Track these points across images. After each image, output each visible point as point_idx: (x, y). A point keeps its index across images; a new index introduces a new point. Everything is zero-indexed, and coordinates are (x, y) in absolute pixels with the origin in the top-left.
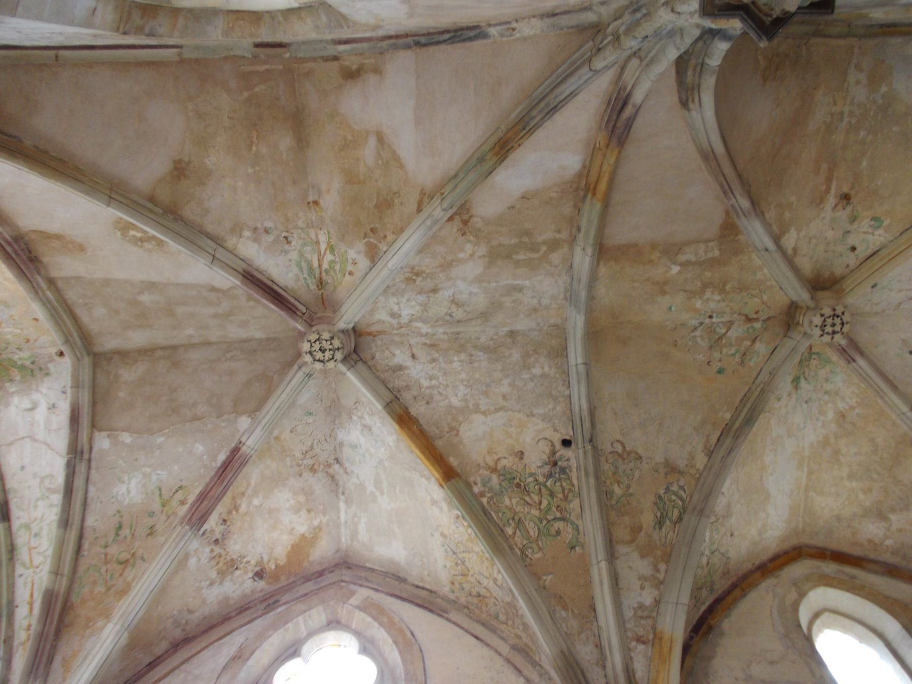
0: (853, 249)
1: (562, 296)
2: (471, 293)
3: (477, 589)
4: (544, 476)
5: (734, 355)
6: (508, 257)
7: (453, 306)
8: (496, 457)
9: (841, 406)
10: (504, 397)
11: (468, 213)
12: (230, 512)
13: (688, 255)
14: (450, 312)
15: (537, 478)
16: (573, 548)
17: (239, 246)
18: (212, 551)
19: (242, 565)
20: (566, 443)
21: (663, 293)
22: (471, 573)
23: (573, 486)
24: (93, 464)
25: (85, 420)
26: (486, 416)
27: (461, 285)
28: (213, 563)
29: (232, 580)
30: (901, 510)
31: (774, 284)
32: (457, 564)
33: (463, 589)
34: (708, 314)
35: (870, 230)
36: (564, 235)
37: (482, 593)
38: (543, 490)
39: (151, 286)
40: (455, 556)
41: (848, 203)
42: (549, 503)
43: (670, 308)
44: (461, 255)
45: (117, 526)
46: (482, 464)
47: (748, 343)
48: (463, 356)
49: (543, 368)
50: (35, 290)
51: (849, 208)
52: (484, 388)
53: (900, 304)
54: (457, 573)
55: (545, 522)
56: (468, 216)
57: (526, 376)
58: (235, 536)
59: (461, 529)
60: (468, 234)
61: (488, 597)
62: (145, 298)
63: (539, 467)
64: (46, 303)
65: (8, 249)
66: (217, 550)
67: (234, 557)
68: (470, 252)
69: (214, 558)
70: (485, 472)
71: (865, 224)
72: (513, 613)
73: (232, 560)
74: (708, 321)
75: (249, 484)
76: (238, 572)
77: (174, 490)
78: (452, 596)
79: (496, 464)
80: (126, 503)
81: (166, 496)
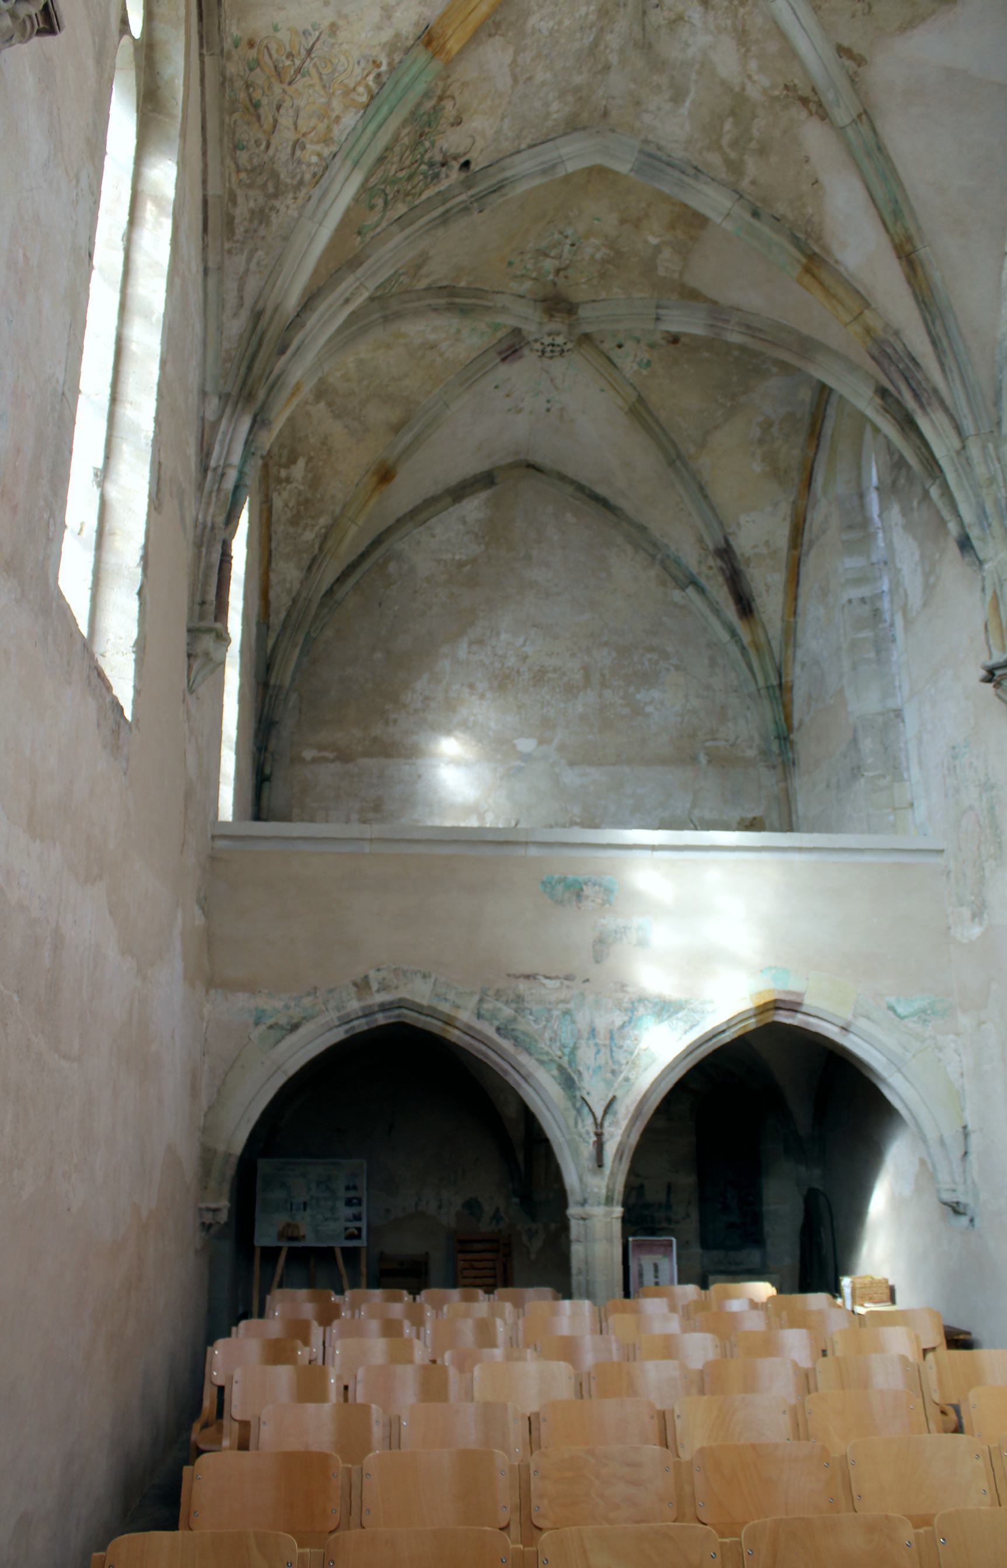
0: (620, 346)
1: (651, 137)
2: (687, 45)
3: (265, 101)
4: (431, 158)
5: (525, 268)
6: (733, 113)
7: (673, 16)
8: (456, 95)
9: (444, 346)
10: (530, 79)
11: (817, 113)
13: (666, 253)
14: (665, 8)
15: (429, 151)
16: (359, 233)
20: (466, 164)
21: (623, 221)
22: (290, 90)
23: (420, 194)
26: (510, 65)
27: (703, 39)
30: (332, 411)
31: (601, 297)
32: (290, 56)
33: (251, 70)
34: (577, 244)
35: (638, 359)
36: (745, 183)
37: (261, 111)
38: (416, 166)
40: (303, 53)
41: (668, 342)
42: (401, 179)
43: (598, 219)
44: (753, 65)
46: (449, 81)
47: (534, 275)
48: (592, 17)
49: (557, 112)
51: (663, 342)
52: (545, 52)
53: (547, 372)
54: (275, 56)
55: (382, 187)
56: (814, 110)
57: (551, 96)
59: (358, 71)
60: (785, 92)
61: (261, 126)
63: (441, 148)
68: (756, 77)
70: (440, 89)
71: (646, 356)
72: (265, 184)
74: (569, 242)
78: (228, 44)
79: (449, 97)
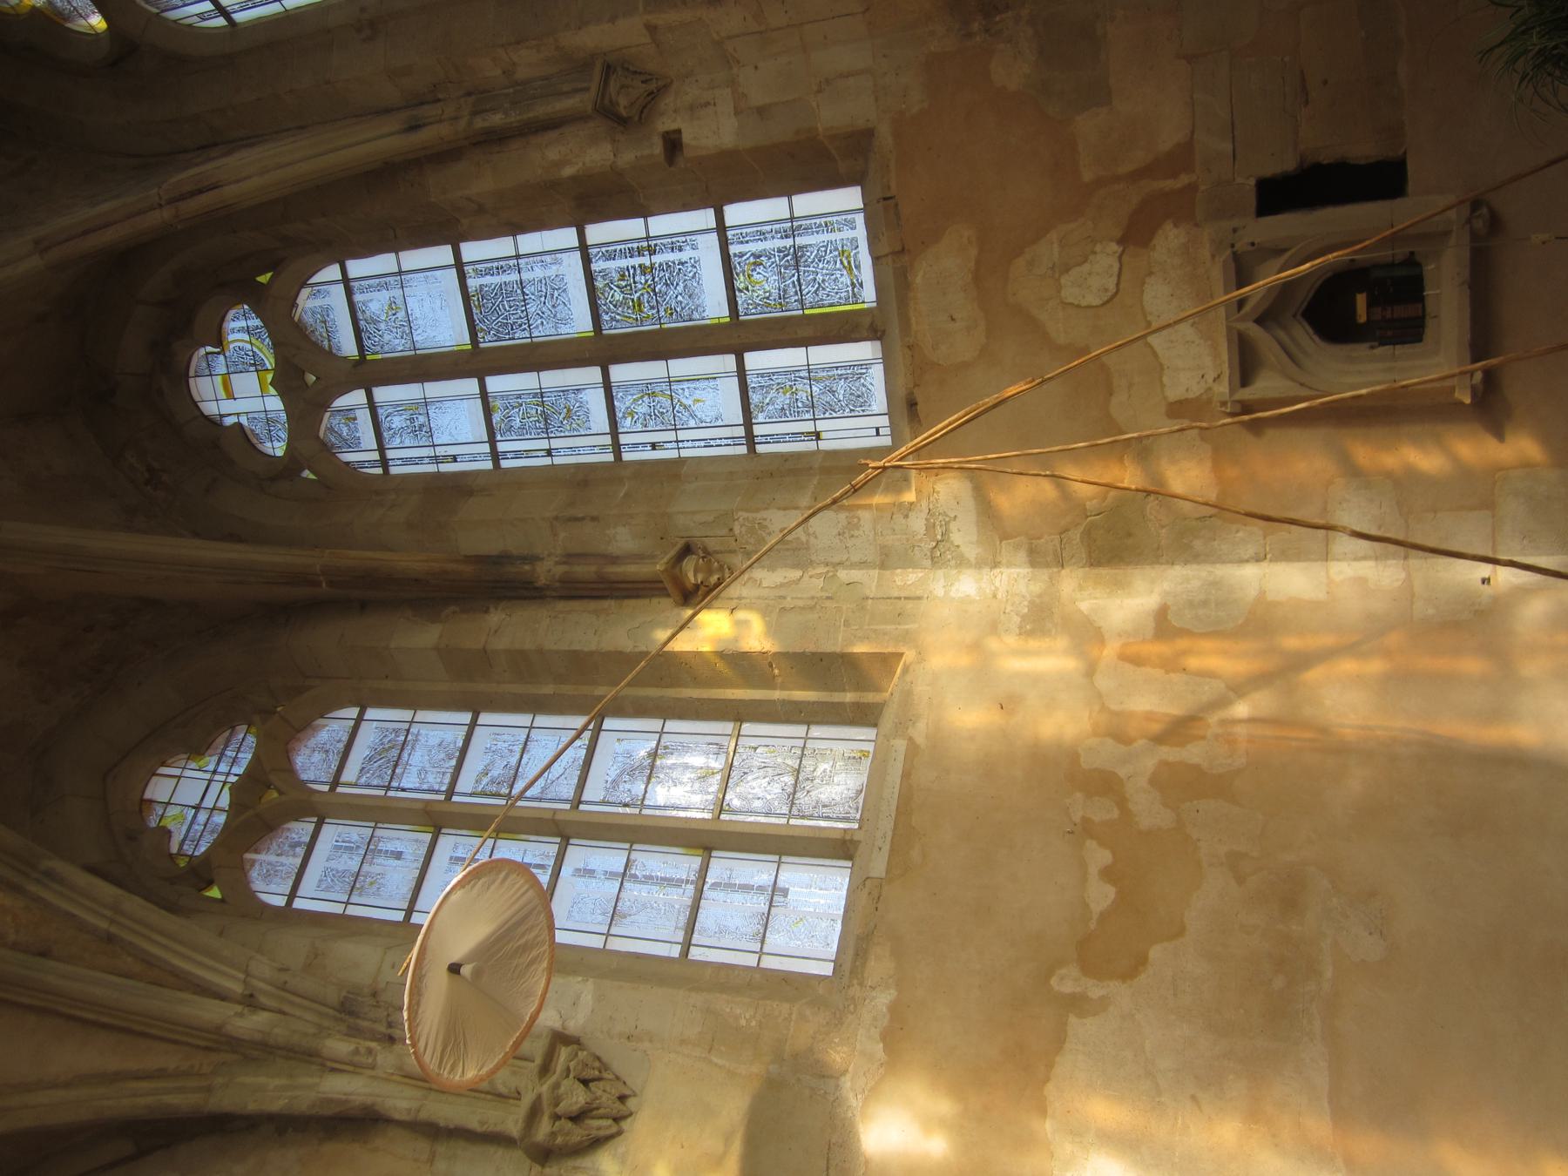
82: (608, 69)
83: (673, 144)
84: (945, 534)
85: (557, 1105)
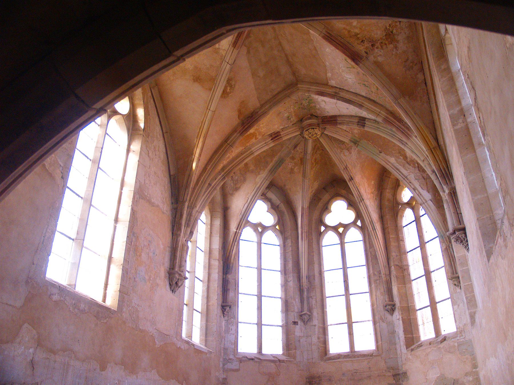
12: (358, 38)
17: (223, 48)
18: (377, 48)
19: (391, 29)
24: (342, 88)
25: (322, 89)
28: (384, 47)
29: (398, 35)
39: (254, 74)
45: (364, 86)
50: (264, 113)
58: (373, 34)
62: (261, 74)
64: (271, 108)
65: (246, 127)
66: (378, 45)
67: (385, 34)
69: (381, 46)
73: (386, 35)
75: (344, 29)
76: (394, 31)
77: (347, 63)
80: (355, 80)
81: (350, 66)
82: (309, 316)
83: (295, 323)
84: (229, 362)
85: (180, 280)
